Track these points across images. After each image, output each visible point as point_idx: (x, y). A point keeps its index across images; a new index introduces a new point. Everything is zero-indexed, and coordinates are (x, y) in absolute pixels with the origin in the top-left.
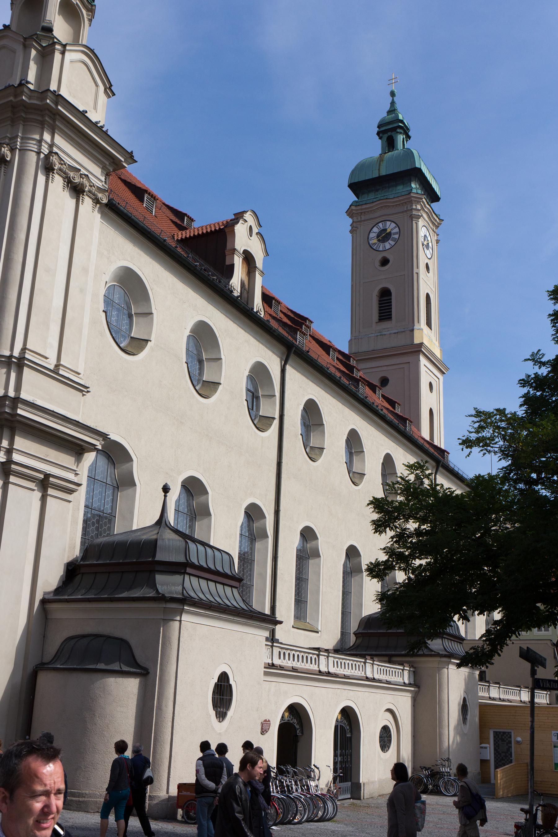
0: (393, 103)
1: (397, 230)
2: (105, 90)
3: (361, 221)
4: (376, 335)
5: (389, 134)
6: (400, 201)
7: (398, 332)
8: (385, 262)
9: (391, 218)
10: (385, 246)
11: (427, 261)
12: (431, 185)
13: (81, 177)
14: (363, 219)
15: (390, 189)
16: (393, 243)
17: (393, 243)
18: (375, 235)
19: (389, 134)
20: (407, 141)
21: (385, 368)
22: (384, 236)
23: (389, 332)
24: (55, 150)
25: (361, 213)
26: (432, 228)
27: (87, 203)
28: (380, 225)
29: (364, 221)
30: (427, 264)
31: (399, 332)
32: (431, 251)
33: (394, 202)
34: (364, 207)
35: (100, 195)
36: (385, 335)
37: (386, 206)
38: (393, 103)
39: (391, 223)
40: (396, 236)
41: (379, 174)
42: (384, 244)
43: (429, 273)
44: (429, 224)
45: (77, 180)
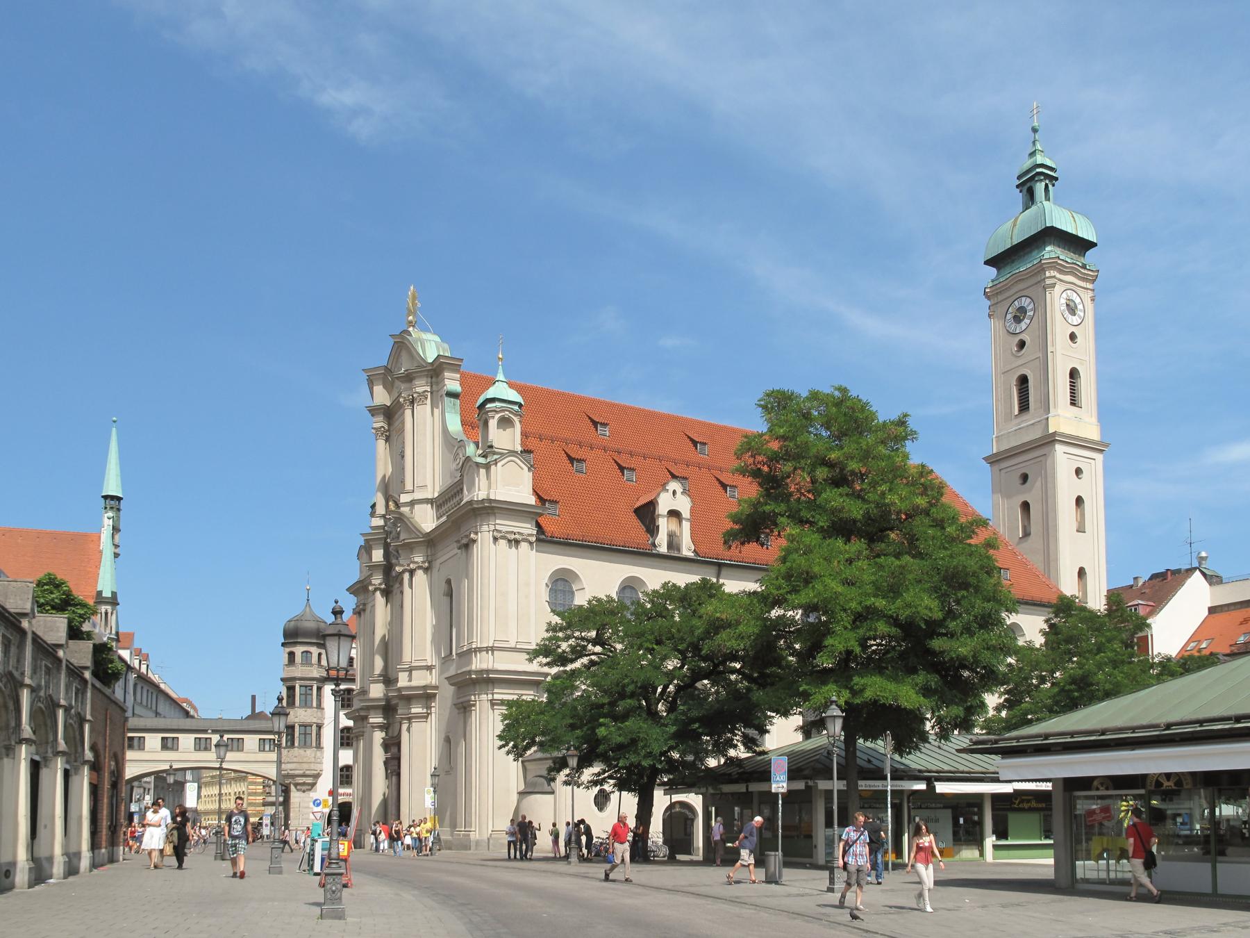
1: (1031, 306)
2: (529, 468)
3: (997, 303)
13: (515, 534)
14: (999, 300)
20: (1053, 185)
24: (498, 527)
25: (997, 293)
27: (524, 545)
28: (1016, 302)
29: (1000, 302)
32: (1082, 314)
34: (998, 286)
35: (530, 538)
44: (1075, 284)
45: (513, 537)
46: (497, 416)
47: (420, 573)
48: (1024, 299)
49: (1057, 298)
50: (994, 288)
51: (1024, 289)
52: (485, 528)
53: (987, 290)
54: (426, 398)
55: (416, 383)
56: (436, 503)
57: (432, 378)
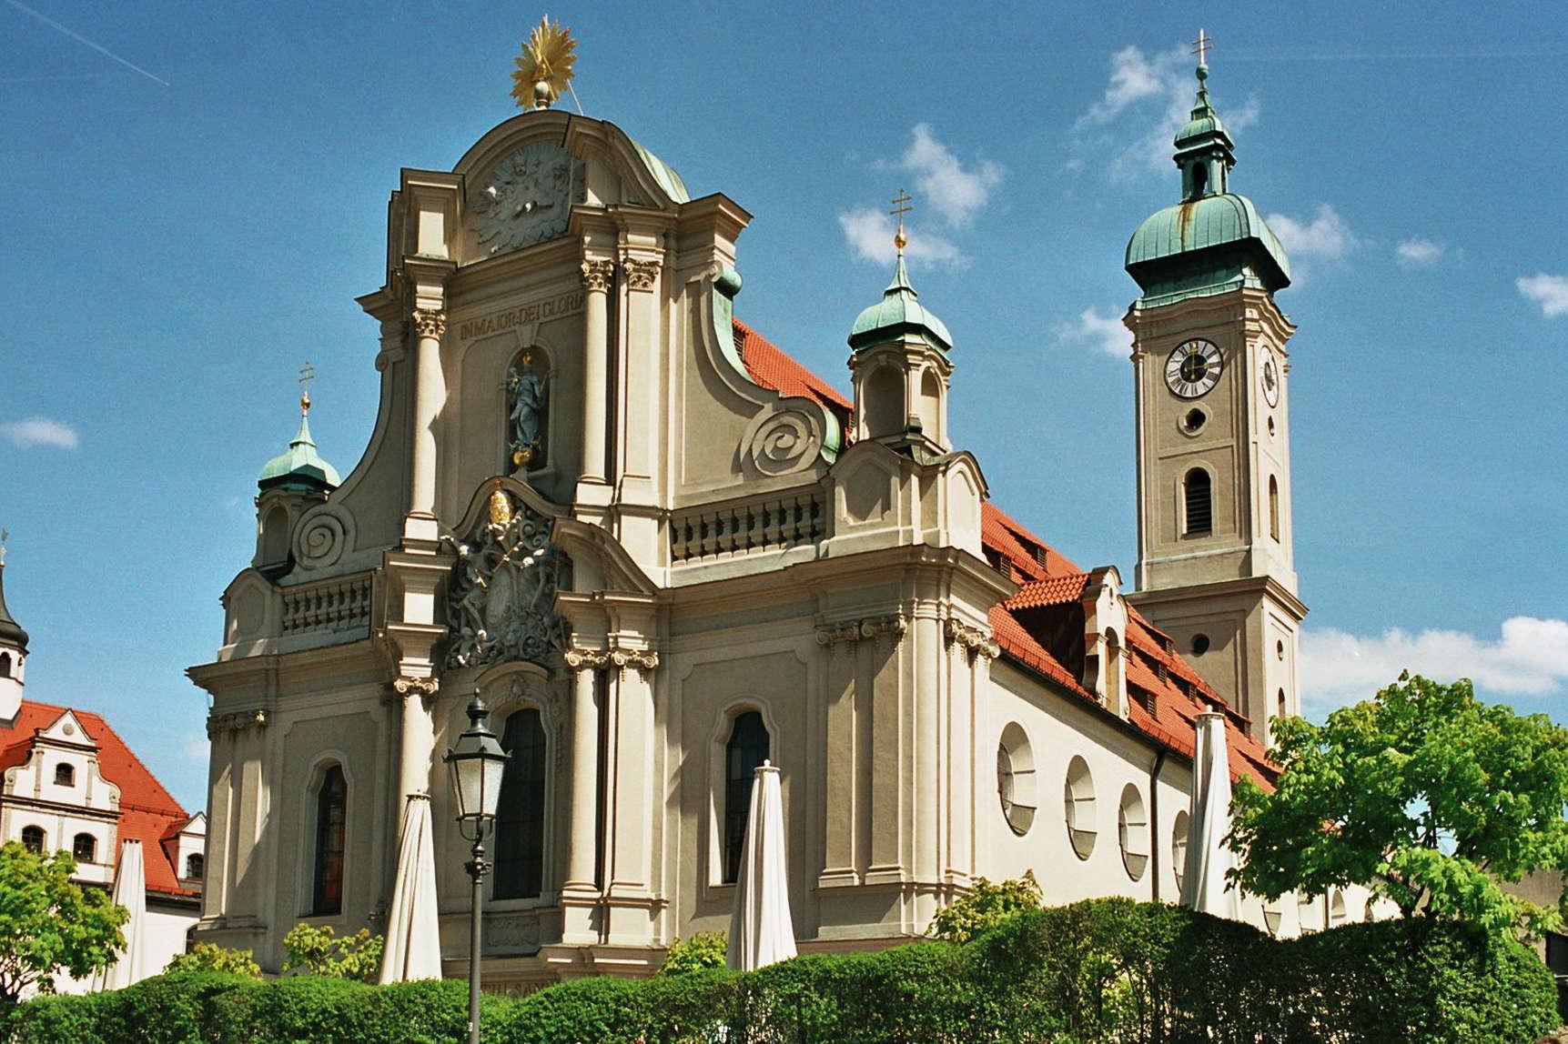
6: (1222, 302)
8: (1196, 419)
9: (1208, 334)
11: (1270, 412)
12: (1275, 263)
15: (1204, 277)
17: (1210, 383)
18: (1178, 366)
21: (1202, 620)
22: (1194, 369)
23: (1207, 553)
26: (1277, 347)
28: (1187, 346)
30: (1270, 419)
33: (1209, 305)
40: (1216, 370)
41: (1183, 247)
43: (1272, 435)
46: (926, 364)
47: (631, 675)
48: (1201, 344)
49: (1259, 353)
50: (1148, 313)
51: (1203, 328)
52: (929, 610)
53: (1137, 314)
54: (653, 279)
55: (630, 237)
56: (671, 522)
57: (665, 236)
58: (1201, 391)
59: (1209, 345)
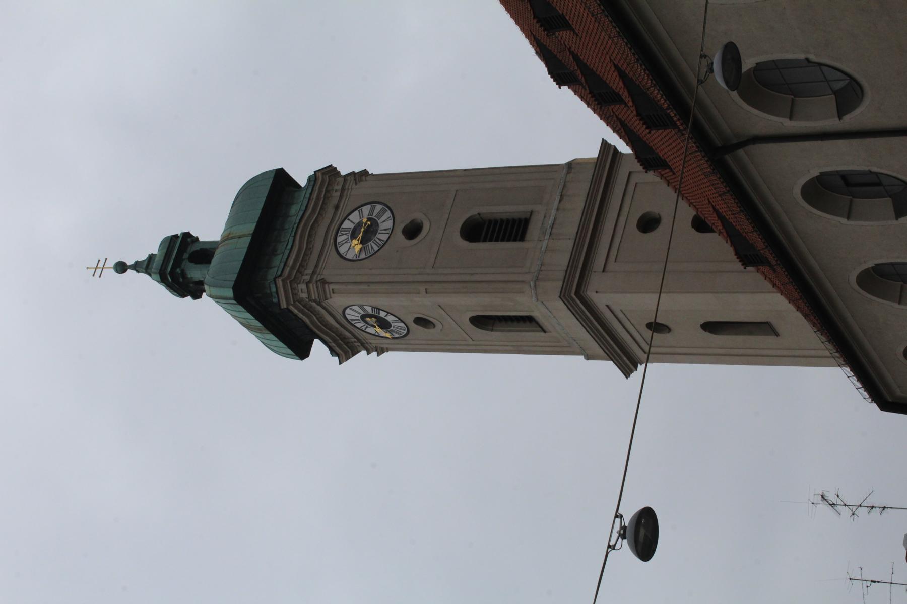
0: (137, 267)
1: (366, 210)
4: (547, 237)
5: (186, 256)
7: (561, 196)
10: (385, 230)
16: (388, 214)
19: (186, 256)
23: (554, 212)
28: (339, 239)
31: (562, 192)
36: (555, 219)
37: (312, 228)
38: (137, 267)
39: (349, 220)
42: (379, 231)
48: (347, 224)
58: (389, 224)
59: (350, 217)
